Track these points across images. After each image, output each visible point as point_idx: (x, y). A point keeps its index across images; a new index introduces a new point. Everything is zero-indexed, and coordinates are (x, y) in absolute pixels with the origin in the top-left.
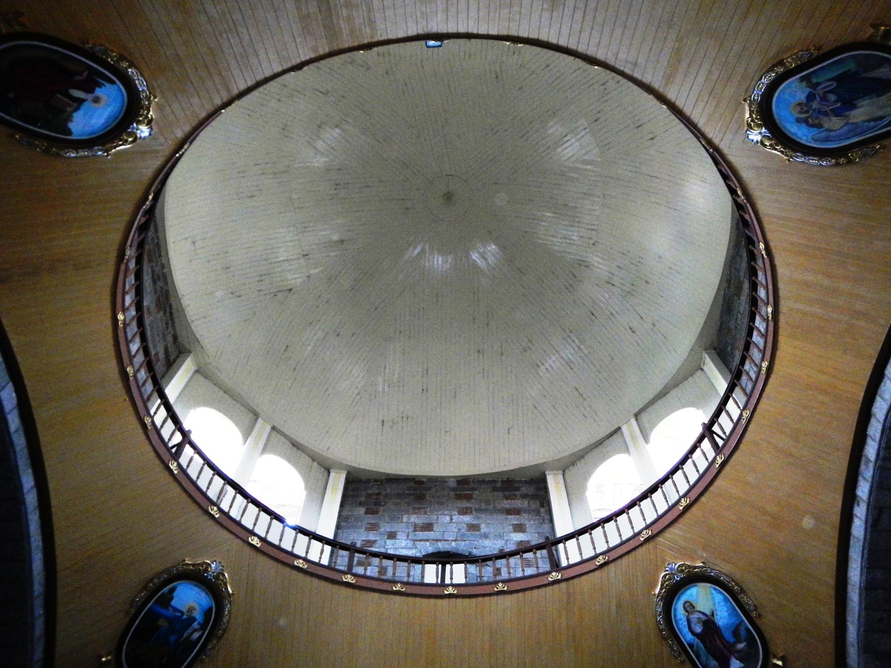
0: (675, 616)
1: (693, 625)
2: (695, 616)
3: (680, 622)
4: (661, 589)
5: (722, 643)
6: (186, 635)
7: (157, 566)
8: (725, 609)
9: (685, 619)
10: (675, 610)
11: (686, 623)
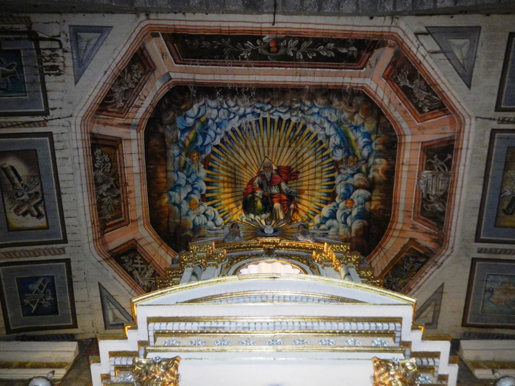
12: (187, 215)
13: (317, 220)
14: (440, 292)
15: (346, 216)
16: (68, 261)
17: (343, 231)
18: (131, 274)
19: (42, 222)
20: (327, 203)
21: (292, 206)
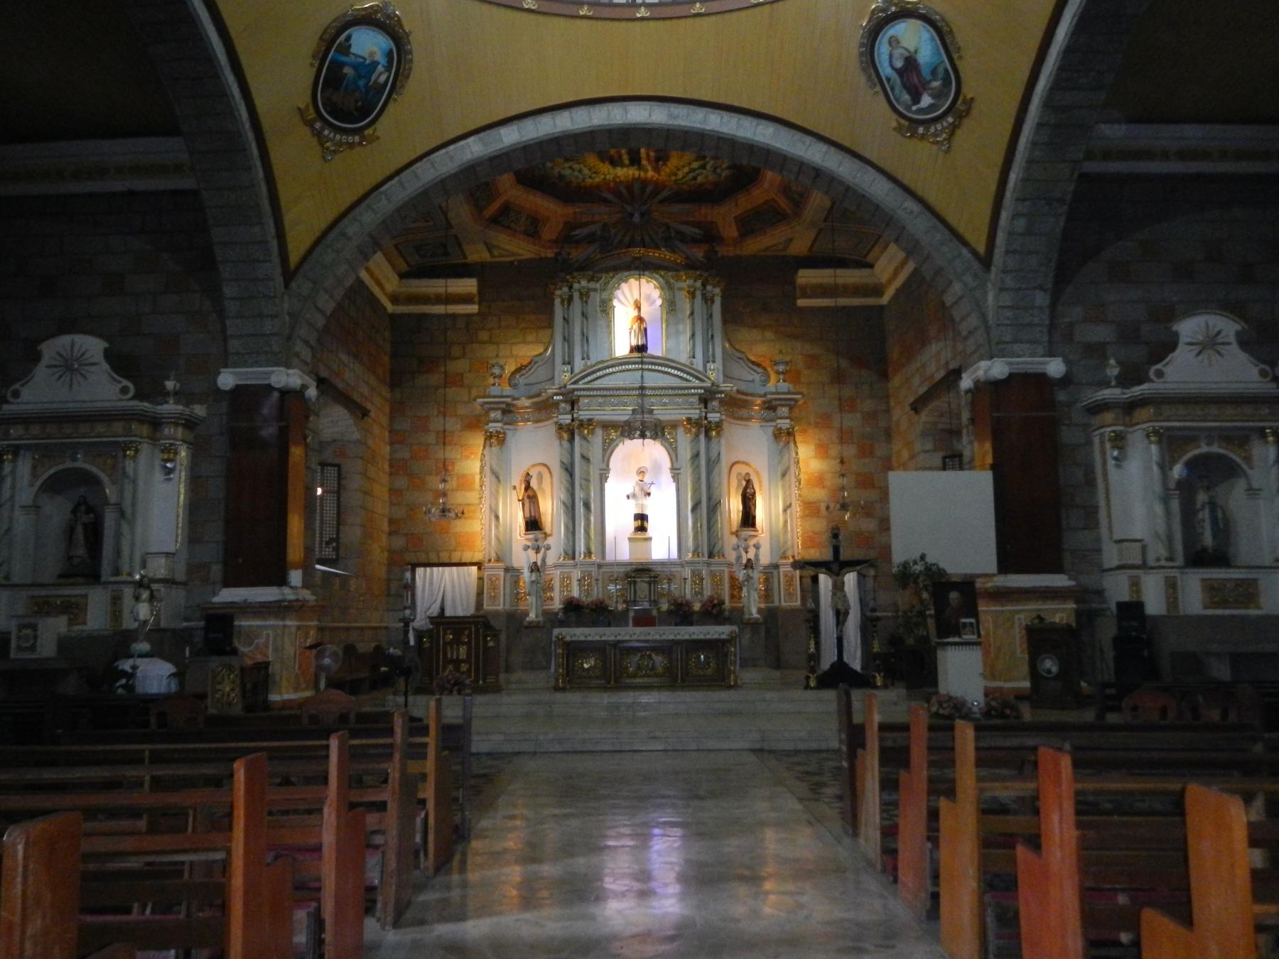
0: (879, 49)
1: (894, 60)
2: (897, 52)
3: (883, 56)
4: (869, 22)
5: (919, 81)
6: (373, 78)
7: (327, 15)
8: (929, 47)
9: (888, 52)
10: (880, 43)
11: (887, 57)
12: (552, 168)
13: (686, 170)
14: (791, 240)
15: (715, 169)
16: (456, 237)
17: (711, 177)
18: (509, 227)
19: (431, 223)
20: (696, 161)
21: (661, 163)
